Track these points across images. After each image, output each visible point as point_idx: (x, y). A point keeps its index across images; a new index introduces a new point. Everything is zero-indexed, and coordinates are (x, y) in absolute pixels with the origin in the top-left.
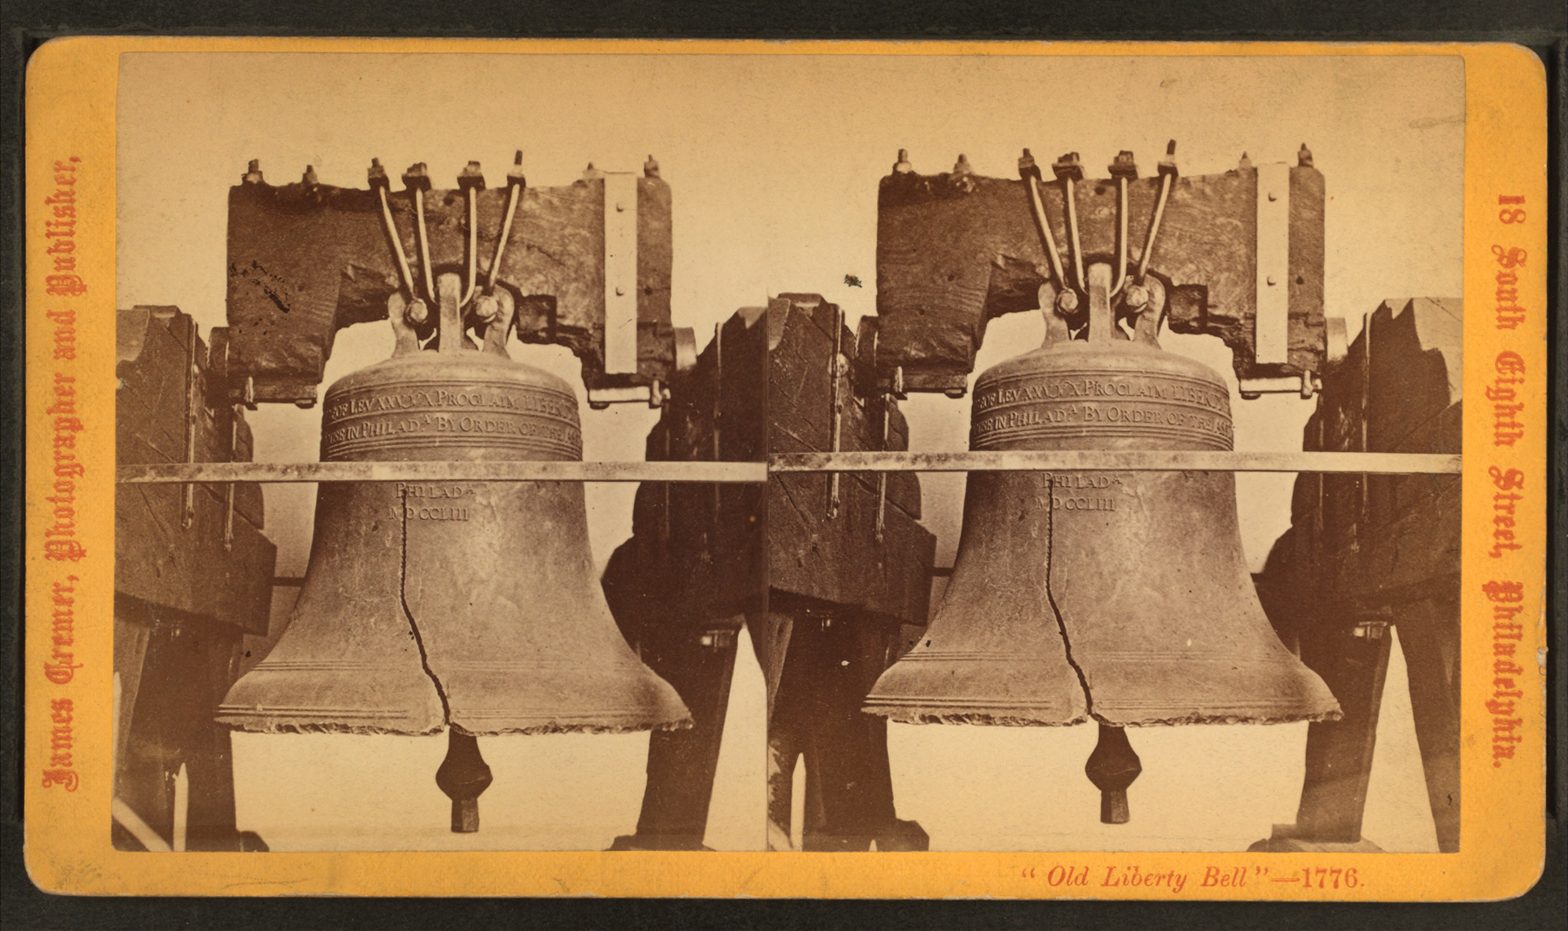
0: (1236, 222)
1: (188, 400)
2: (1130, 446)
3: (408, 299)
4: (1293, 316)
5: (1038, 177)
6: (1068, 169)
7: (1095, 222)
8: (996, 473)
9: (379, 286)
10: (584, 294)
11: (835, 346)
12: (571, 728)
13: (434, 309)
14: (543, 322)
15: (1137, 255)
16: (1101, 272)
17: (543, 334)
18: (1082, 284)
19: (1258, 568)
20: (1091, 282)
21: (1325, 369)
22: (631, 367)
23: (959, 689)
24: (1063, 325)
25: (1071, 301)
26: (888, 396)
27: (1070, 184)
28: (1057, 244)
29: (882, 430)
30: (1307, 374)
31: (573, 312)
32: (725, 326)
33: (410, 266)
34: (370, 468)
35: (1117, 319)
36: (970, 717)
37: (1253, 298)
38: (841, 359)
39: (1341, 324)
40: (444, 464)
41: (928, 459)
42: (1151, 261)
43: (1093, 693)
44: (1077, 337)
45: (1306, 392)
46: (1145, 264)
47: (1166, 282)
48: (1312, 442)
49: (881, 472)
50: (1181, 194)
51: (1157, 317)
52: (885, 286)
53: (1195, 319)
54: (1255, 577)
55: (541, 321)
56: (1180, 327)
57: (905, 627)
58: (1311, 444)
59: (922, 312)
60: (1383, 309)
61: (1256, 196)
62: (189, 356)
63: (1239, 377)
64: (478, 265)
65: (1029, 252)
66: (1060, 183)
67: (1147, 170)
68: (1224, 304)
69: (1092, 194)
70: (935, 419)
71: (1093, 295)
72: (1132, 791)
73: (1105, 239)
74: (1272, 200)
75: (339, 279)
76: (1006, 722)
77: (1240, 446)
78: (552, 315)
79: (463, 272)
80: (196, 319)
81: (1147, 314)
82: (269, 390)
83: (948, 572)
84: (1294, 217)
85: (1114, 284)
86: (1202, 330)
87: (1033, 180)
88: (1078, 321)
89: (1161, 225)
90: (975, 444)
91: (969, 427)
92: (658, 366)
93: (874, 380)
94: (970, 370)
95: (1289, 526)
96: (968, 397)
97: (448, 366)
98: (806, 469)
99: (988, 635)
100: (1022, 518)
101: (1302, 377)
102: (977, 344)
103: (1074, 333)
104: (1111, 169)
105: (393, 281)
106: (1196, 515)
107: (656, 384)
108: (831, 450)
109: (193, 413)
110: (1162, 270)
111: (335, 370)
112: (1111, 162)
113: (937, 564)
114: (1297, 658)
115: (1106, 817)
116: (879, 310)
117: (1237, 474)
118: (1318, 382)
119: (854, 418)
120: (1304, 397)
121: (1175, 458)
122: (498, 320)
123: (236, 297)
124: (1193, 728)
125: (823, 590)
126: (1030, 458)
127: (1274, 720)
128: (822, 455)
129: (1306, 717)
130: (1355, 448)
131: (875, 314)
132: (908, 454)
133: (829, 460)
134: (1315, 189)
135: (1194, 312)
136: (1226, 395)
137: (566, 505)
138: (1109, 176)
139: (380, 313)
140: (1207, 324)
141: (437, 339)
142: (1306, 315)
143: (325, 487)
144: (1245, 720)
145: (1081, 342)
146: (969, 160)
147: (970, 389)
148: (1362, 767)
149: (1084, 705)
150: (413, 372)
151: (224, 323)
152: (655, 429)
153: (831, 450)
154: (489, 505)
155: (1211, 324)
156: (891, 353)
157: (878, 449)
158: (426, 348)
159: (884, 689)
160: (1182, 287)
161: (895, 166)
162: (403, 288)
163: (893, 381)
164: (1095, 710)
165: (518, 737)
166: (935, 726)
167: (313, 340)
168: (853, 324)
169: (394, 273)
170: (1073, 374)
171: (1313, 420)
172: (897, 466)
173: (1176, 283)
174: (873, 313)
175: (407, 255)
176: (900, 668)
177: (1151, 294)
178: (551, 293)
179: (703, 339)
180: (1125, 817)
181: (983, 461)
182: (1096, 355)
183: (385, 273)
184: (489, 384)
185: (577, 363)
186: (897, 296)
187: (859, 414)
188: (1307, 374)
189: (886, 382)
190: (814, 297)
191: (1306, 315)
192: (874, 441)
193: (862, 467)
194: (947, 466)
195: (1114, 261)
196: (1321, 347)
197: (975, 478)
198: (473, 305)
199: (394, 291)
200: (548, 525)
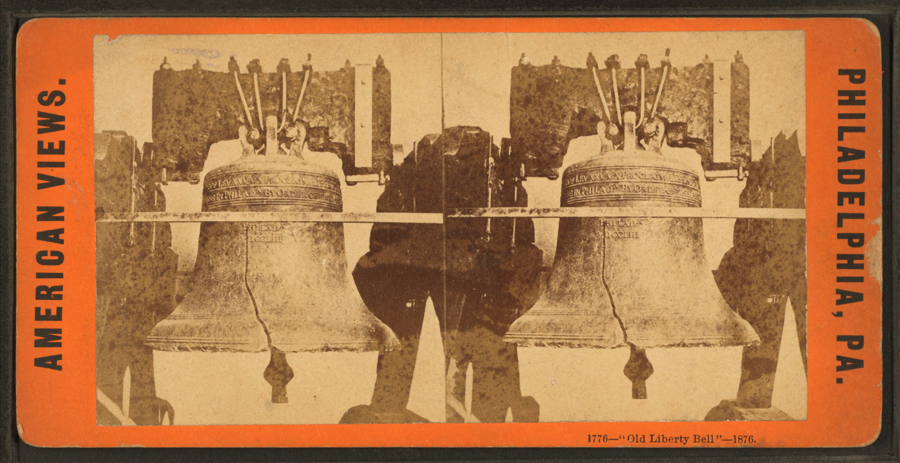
4: (732, 138)
5: (597, 67)
12: (336, 349)
13: (263, 132)
14: (322, 141)
15: (649, 106)
16: (630, 116)
20: (625, 121)
22: (369, 165)
28: (607, 100)
31: (338, 135)
33: (251, 111)
35: (639, 140)
36: (562, 344)
37: (711, 130)
38: (491, 160)
39: (759, 143)
40: (269, 213)
41: (539, 212)
43: (627, 332)
45: (741, 177)
47: (665, 120)
49: (513, 218)
55: (318, 139)
60: (781, 136)
67: (654, 64)
68: (696, 130)
70: (542, 192)
71: (626, 128)
76: (580, 346)
80: (136, 137)
82: (174, 175)
85: (637, 123)
87: (594, 69)
90: (562, 205)
94: (561, 165)
99: (571, 302)
102: (564, 153)
103: (616, 147)
104: (637, 64)
106: (682, 239)
107: (382, 173)
108: (487, 206)
112: (635, 59)
118: (747, 173)
129: (741, 344)
132: (528, 209)
136: (697, 179)
138: (634, 67)
139: (236, 136)
142: (740, 138)
143: (205, 226)
150: (252, 166)
153: (487, 206)
154: (292, 235)
158: (259, 153)
159: (514, 330)
163: (519, 171)
165: (308, 353)
166: (542, 348)
168: (498, 143)
170: (617, 168)
173: (671, 121)
174: (510, 137)
175: (249, 106)
176: (525, 318)
177: (657, 127)
180: (644, 396)
181: (567, 212)
184: (293, 172)
185: (340, 162)
190: (478, 128)
191: (739, 138)
192: (510, 202)
193: (503, 215)
195: (636, 109)
196: (748, 154)
198: (284, 131)
199: (242, 124)
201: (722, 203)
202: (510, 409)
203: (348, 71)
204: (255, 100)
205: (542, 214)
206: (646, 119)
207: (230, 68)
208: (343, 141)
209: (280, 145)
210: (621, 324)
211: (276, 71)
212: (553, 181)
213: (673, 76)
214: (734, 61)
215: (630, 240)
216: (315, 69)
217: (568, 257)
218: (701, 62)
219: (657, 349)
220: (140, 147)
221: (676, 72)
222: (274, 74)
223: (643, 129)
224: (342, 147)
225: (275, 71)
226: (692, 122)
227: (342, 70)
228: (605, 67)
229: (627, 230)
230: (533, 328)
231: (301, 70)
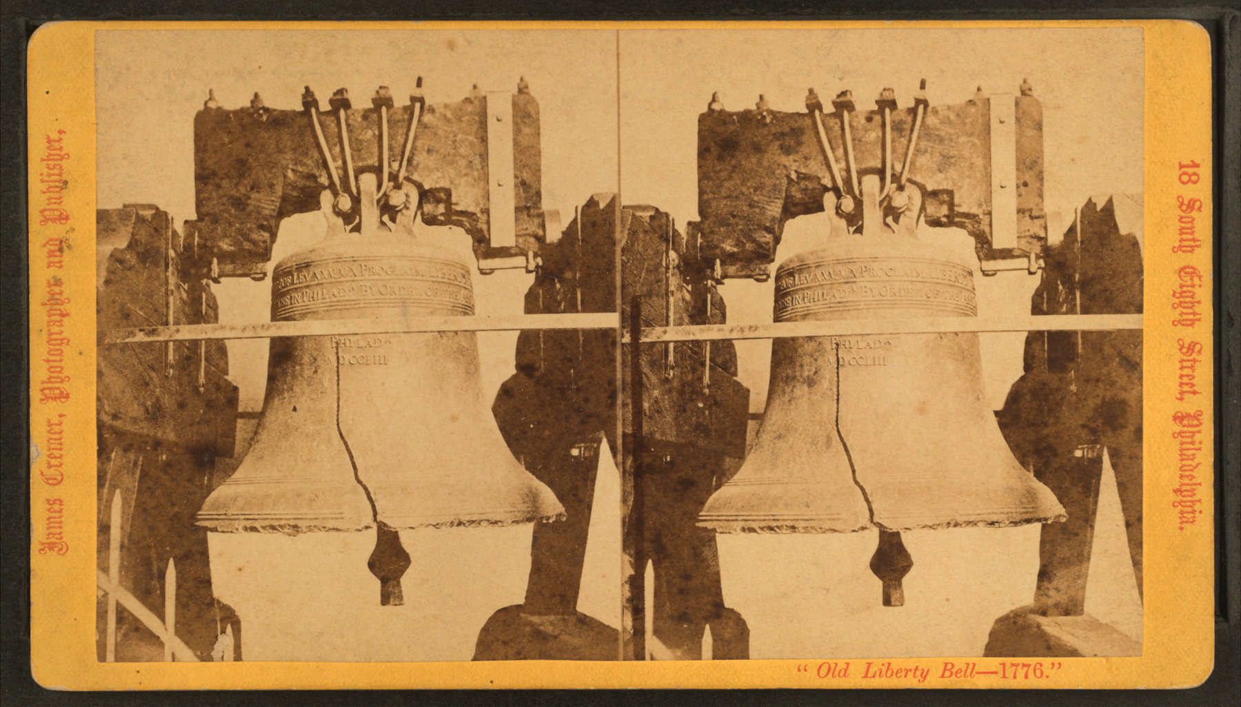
1: (167, 278)
3: (336, 194)
5: (821, 110)
7: (866, 143)
8: (793, 339)
9: (312, 184)
13: (356, 200)
14: (441, 208)
15: (898, 168)
16: (871, 182)
17: (442, 218)
19: (1000, 406)
20: (864, 191)
21: (1047, 252)
25: (848, 204)
26: (710, 282)
27: (846, 114)
30: (1033, 256)
31: (465, 199)
33: (337, 168)
35: (886, 215)
41: (742, 330)
43: (874, 506)
44: (855, 232)
45: (1032, 270)
47: (922, 188)
48: (1036, 310)
50: (931, 120)
52: (705, 197)
54: (997, 413)
55: (437, 206)
56: (935, 223)
57: (727, 459)
58: (1036, 310)
60: (1090, 204)
62: (167, 244)
63: (980, 259)
64: (390, 166)
65: (815, 167)
66: (838, 115)
67: (904, 102)
68: (966, 203)
69: (863, 121)
71: (866, 200)
72: (907, 580)
73: (874, 156)
75: (281, 179)
76: (806, 530)
79: (378, 170)
82: (229, 268)
92: (532, 240)
93: (697, 268)
94: (773, 261)
95: (1023, 373)
96: (772, 281)
100: (816, 373)
101: (1029, 257)
102: (777, 240)
103: (852, 229)
105: (324, 180)
106: (950, 366)
107: (531, 254)
109: (171, 287)
110: (918, 179)
112: (877, 97)
113: (752, 410)
114: (1032, 474)
115: (887, 602)
116: (701, 213)
117: (982, 337)
118: (1042, 262)
119: (683, 299)
120: (1030, 273)
121: (932, 324)
122: (407, 208)
124: (951, 529)
125: (663, 434)
127: (1016, 523)
128: (659, 330)
129: (1039, 520)
130: (1071, 311)
131: (697, 219)
133: (665, 332)
134: (1035, 114)
136: (971, 274)
137: (465, 352)
138: (876, 108)
141: (360, 223)
142: (1031, 210)
144: (992, 523)
145: (858, 235)
146: (766, 98)
147: (773, 275)
148: (1082, 557)
149: (867, 515)
150: (341, 250)
151: (193, 216)
152: (530, 289)
159: (712, 508)
161: (710, 105)
162: (332, 186)
164: (876, 519)
169: (324, 173)
171: (1037, 290)
175: (334, 160)
178: (447, 186)
181: (785, 330)
185: (469, 240)
186: (714, 204)
188: (1033, 256)
192: (698, 314)
193: (691, 337)
195: (881, 172)
196: (1042, 234)
199: (325, 188)
200: (450, 365)
202: (708, 627)
203: (476, 102)
204: (342, 149)
206: (895, 185)
207: (305, 104)
208: (471, 209)
209: (381, 215)
210: (864, 493)
211: (371, 106)
212: (763, 284)
213: (931, 120)
214: (1018, 94)
216: (428, 102)
217: (787, 398)
219: (917, 532)
220: (179, 226)
221: (935, 112)
222: (370, 110)
224: (474, 214)
225: (371, 106)
226: (960, 188)
227: (468, 100)
228: (833, 110)
230: (739, 505)
231: (408, 103)
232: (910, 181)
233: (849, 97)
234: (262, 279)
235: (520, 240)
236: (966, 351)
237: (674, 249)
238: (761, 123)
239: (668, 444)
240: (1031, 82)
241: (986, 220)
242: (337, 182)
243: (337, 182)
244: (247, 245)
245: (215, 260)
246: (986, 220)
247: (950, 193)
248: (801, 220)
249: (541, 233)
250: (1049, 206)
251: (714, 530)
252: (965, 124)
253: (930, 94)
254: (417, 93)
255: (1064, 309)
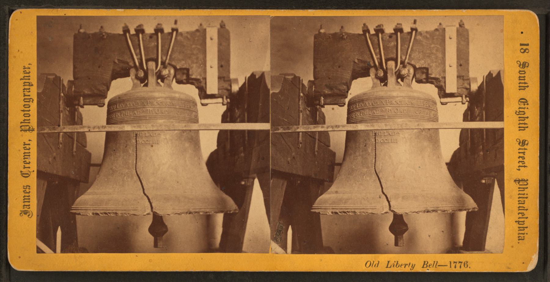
0: (438, 46)
2: (403, 121)
3: (137, 70)
5: (369, 32)
6: (379, 30)
7: (389, 47)
8: (356, 131)
10: (199, 68)
11: (299, 90)
14: (185, 77)
15: (404, 58)
16: (391, 64)
18: (385, 68)
20: (388, 67)
23: (345, 203)
24: (379, 82)
25: (381, 74)
26: (318, 106)
27: (380, 35)
28: (376, 55)
29: (316, 117)
30: (464, 96)
32: (249, 78)
33: (138, 59)
34: (124, 127)
35: (397, 79)
37: (444, 71)
39: (475, 79)
41: (332, 127)
42: (409, 59)
43: (391, 203)
44: (384, 85)
45: (464, 102)
46: (407, 61)
47: (414, 67)
48: (465, 119)
49: (316, 132)
51: (411, 78)
53: (424, 79)
56: (419, 81)
59: (329, 78)
60: (490, 74)
61: (445, 37)
65: (367, 58)
69: (388, 38)
71: (389, 71)
74: (450, 38)
77: (440, 120)
78: (188, 75)
81: (407, 77)
82: (88, 101)
83: (340, 165)
84: (458, 43)
86: (427, 82)
88: (384, 80)
89: (412, 48)
90: (349, 121)
91: (346, 116)
92: (225, 91)
94: (346, 97)
96: (346, 106)
97: (151, 92)
98: (290, 131)
99: (354, 185)
100: (365, 146)
101: (462, 97)
102: (349, 89)
103: (382, 84)
104: (394, 30)
105: (131, 64)
106: (426, 143)
107: (225, 97)
110: (413, 62)
111: (111, 94)
113: (337, 162)
116: (314, 77)
120: (463, 104)
121: (418, 125)
123: (76, 70)
126: (368, 126)
132: (325, 126)
133: (298, 128)
135: (424, 76)
136: (435, 103)
137: (193, 139)
138: (393, 32)
139: (127, 75)
140: (428, 80)
142: (463, 76)
145: (385, 87)
147: (347, 103)
150: (139, 95)
152: (224, 113)
155: (430, 80)
156: (319, 92)
157: (315, 124)
158: (144, 86)
160: (420, 68)
162: (135, 66)
163: (320, 101)
167: (104, 84)
170: (381, 98)
172: (322, 130)
173: (417, 67)
174: (312, 79)
175: (136, 55)
176: (324, 196)
177: (409, 71)
179: (241, 82)
181: (351, 127)
182: (390, 91)
183: (129, 61)
184: (166, 98)
185: (197, 91)
187: (308, 112)
188: (464, 96)
189: (318, 102)
191: (463, 77)
193: (310, 130)
194: (339, 129)
196: (468, 87)
197: (348, 132)
198: (160, 71)
199: (132, 67)
201: (452, 120)
205: (336, 129)
209: (158, 79)
210: (387, 198)
211: (153, 32)
213: (419, 37)
214: (458, 26)
215: (392, 144)
216: (180, 31)
218: (437, 28)
221: (421, 34)
223: (399, 73)
229: (390, 138)
231: (170, 31)
232: (409, 63)
233: (382, 27)
234: (103, 106)
235: (220, 91)
236: (432, 137)
237: (302, 92)
238: (342, 38)
239: (299, 176)
240: (465, 22)
241: (443, 80)
242: (137, 64)
243: (137, 64)
244: (96, 91)
245: (82, 98)
246: (443, 80)
247: (427, 69)
248: (360, 80)
249: (229, 88)
250: (471, 75)
251: (319, 213)
252: (433, 39)
253: (417, 26)
254: (174, 26)
255: (478, 119)
